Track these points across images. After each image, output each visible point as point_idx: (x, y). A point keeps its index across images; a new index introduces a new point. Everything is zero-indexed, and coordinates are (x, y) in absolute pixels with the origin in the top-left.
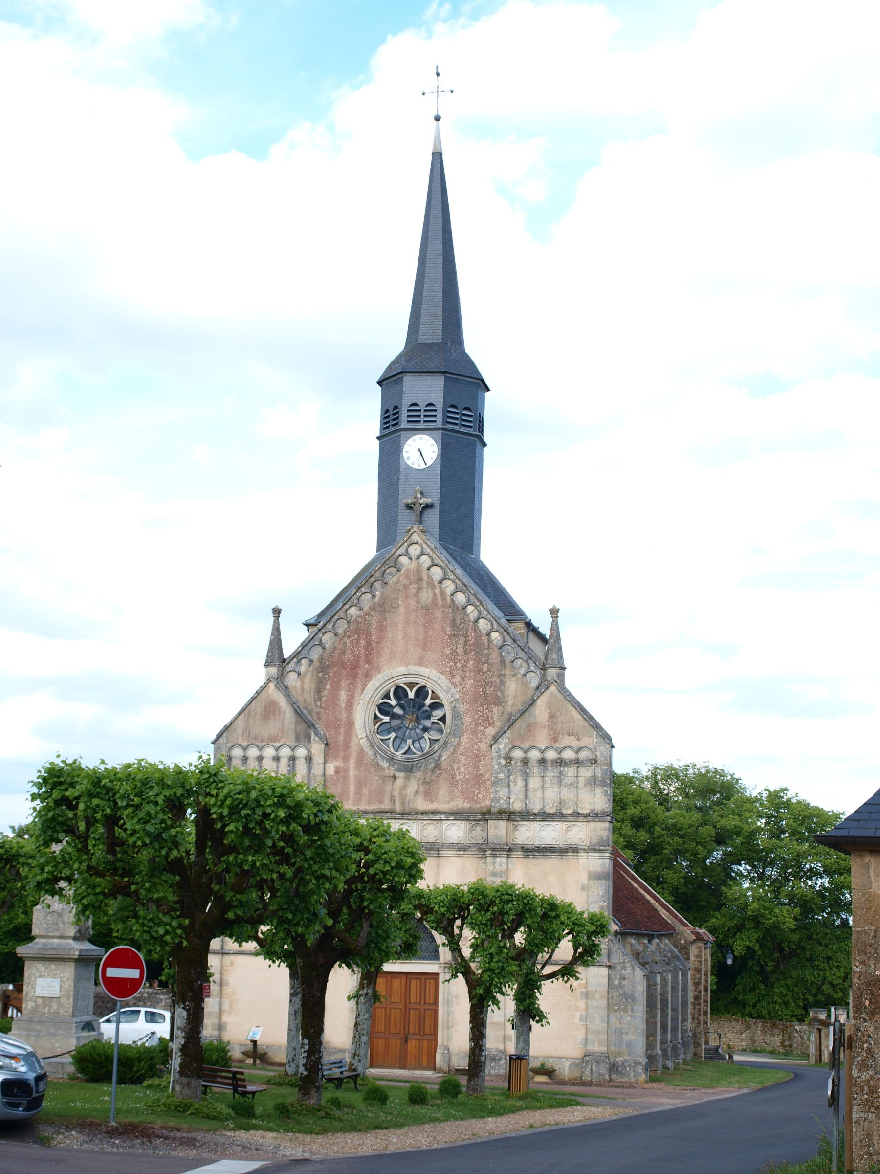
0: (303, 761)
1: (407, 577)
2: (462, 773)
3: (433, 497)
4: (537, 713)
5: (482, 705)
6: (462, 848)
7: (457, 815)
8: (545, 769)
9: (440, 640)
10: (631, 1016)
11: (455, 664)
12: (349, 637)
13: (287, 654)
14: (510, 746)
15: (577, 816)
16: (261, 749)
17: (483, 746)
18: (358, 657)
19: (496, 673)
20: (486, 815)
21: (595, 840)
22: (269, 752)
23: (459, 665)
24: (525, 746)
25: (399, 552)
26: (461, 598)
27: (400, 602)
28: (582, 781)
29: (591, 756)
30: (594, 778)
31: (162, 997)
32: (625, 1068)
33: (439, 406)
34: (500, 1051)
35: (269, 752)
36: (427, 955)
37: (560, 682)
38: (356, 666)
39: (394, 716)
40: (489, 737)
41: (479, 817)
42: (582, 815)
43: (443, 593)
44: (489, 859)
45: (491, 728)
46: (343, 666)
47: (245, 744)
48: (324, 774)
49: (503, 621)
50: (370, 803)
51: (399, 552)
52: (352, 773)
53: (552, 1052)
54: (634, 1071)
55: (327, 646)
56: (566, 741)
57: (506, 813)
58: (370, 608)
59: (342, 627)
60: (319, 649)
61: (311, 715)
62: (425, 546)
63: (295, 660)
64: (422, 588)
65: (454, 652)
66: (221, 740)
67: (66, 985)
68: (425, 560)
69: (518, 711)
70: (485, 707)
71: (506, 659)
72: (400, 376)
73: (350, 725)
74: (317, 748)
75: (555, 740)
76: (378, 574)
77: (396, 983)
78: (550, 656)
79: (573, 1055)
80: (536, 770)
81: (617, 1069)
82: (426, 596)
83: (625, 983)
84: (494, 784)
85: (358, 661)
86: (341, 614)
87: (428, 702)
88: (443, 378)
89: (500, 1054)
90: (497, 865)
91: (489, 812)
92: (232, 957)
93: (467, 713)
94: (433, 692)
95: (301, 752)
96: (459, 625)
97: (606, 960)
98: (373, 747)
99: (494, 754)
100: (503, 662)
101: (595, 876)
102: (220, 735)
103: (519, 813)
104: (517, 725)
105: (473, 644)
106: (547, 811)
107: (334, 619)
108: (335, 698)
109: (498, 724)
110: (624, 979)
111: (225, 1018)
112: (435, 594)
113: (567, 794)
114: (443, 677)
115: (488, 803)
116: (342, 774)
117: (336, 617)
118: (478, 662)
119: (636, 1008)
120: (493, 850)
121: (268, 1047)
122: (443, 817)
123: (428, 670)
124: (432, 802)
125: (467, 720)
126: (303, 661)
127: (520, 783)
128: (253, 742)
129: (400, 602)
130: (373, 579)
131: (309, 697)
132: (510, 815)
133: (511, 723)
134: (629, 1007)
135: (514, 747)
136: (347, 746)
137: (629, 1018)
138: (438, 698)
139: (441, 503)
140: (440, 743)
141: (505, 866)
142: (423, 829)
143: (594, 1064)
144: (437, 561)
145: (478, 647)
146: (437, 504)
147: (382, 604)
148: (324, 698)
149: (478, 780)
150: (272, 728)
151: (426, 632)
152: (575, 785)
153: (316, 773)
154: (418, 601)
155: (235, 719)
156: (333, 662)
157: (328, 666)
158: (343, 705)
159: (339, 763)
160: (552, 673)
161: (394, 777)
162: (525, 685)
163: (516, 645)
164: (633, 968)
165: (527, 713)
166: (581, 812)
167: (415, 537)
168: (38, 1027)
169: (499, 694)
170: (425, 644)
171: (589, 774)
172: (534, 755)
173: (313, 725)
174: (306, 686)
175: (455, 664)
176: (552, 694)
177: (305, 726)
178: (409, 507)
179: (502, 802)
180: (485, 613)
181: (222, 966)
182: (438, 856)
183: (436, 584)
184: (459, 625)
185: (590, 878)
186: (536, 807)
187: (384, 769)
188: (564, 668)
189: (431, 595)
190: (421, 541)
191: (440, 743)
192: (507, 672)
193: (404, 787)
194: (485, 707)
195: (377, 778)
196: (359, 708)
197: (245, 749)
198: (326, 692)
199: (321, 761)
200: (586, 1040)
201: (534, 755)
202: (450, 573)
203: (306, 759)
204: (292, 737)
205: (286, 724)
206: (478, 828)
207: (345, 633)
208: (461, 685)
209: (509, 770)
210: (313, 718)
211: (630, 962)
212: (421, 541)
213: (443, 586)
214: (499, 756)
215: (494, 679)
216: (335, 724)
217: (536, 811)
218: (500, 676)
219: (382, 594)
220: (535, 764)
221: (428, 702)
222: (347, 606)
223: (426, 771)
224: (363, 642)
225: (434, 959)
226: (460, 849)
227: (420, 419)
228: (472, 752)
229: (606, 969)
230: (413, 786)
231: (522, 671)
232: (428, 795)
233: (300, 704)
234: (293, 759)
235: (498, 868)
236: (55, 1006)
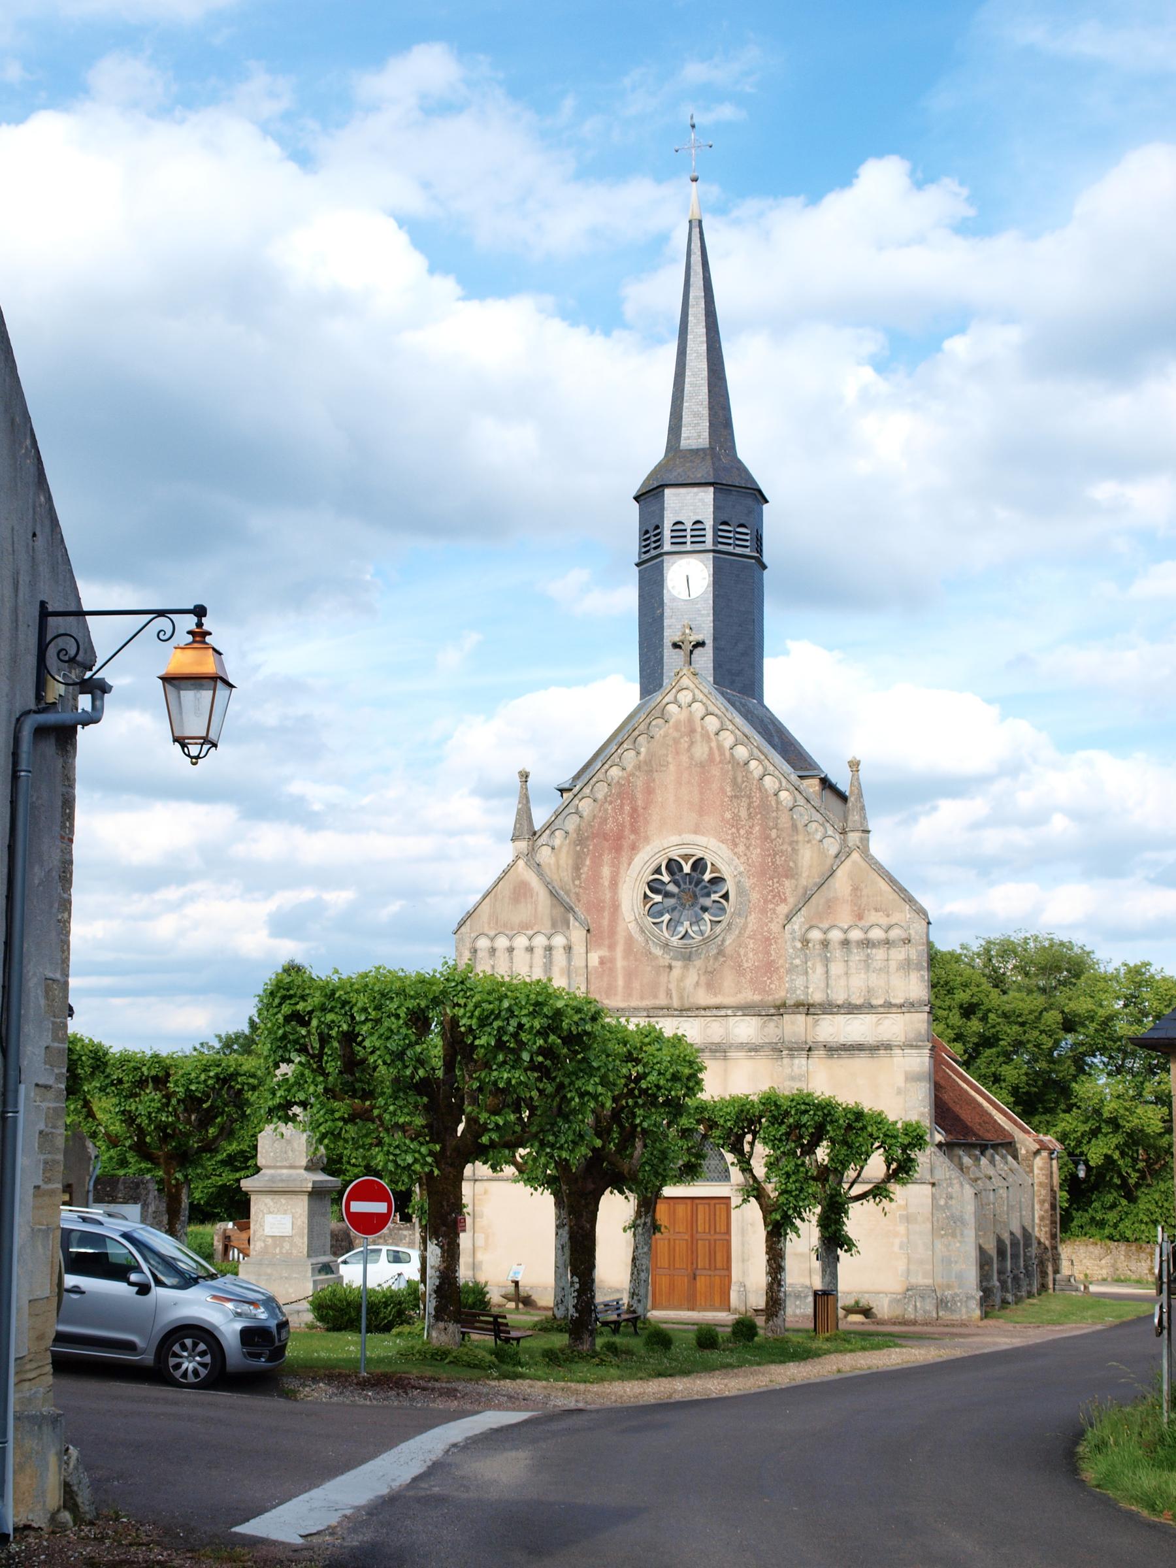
0: (561, 951)
1: (677, 728)
2: (750, 959)
3: (705, 631)
4: (837, 885)
5: (771, 878)
6: (753, 1049)
7: (747, 1010)
8: (849, 951)
11: (738, 830)
12: (611, 803)
14: (807, 926)
15: (888, 1005)
17: (775, 927)
18: (623, 825)
20: (780, 1009)
21: (912, 1035)
22: (521, 942)
24: (825, 925)
26: (742, 752)
27: (670, 759)
28: (893, 965)
29: (904, 935)
30: (908, 961)
31: (405, 1233)
32: (955, 1303)
33: (709, 524)
35: (521, 942)
37: (864, 850)
38: (620, 837)
39: (667, 895)
41: (772, 1011)
42: (895, 1005)
43: (720, 747)
44: (786, 1061)
45: (783, 905)
46: (605, 837)
47: (492, 933)
49: (794, 777)
50: (642, 998)
52: (620, 963)
54: (967, 1307)
55: (585, 814)
56: (873, 917)
57: (803, 1005)
58: (634, 767)
59: (601, 791)
62: (697, 691)
65: (736, 817)
66: (463, 929)
67: (299, 1222)
69: (815, 884)
73: (616, 907)
74: (577, 935)
75: (860, 917)
76: (642, 727)
77: (681, 1209)
82: (701, 751)
83: (953, 1202)
84: (789, 971)
85: (623, 830)
86: (600, 775)
87: (707, 876)
90: (795, 1068)
91: (784, 1005)
95: (559, 941)
97: (928, 1177)
98: (643, 932)
99: (787, 936)
100: (794, 827)
101: (911, 1078)
102: (462, 924)
105: (758, 806)
107: (592, 782)
108: (596, 877)
110: (951, 1198)
111: (480, 1256)
112: (711, 749)
113: (875, 980)
114: (723, 846)
115: (783, 994)
116: (608, 965)
117: (594, 779)
118: (765, 828)
119: (966, 1232)
120: (791, 1050)
122: (729, 1012)
124: (715, 995)
125: (755, 896)
126: (557, 833)
127: (820, 969)
130: (636, 733)
131: (566, 875)
132: (808, 1008)
134: (958, 1231)
135: (811, 927)
136: (612, 932)
138: (718, 871)
139: (715, 639)
141: (804, 1068)
142: (706, 1027)
144: (712, 708)
145: (764, 808)
147: (648, 763)
149: (769, 967)
150: (523, 913)
151: (701, 793)
152: (885, 970)
154: (691, 758)
158: (607, 884)
160: (854, 838)
162: (822, 853)
164: (962, 1185)
165: (825, 886)
166: (894, 1001)
167: (685, 681)
168: (269, 1271)
169: (791, 864)
172: (836, 935)
173: (572, 908)
174: (562, 862)
175: (738, 830)
176: (854, 863)
177: (562, 909)
178: (676, 646)
179: (798, 992)
180: (772, 768)
182: (725, 1058)
184: (740, 785)
185: (907, 1079)
186: (839, 997)
188: (868, 832)
189: (706, 749)
190: (692, 686)
191: (724, 925)
192: (801, 838)
193: (682, 979)
195: (649, 968)
197: (492, 939)
198: (586, 869)
199: (583, 950)
200: (908, 1271)
201: (836, 935)
202: (728, 723)
204: (548, 924)
205: (540, 908)
206: (772, 1025)
209: (806, 955)
210: (571, 900)
211: (958, 1178)
212: (692, 686)
213: (721, 738)
214: (794, 939)
216: (596, 907)
217: (839, 1002)
218: (791, 843)
219: (648, 749)
220: (837, 946)
221: (707, 876)
222: (606, 766)
223: (707, 958)
224: (627, 808)
227: (687, 538)
230: (692, 977)
231: (819, 836)
232: (710, 986)
233: (555, 884)
234: (549, 949)
236: (287, 1246)
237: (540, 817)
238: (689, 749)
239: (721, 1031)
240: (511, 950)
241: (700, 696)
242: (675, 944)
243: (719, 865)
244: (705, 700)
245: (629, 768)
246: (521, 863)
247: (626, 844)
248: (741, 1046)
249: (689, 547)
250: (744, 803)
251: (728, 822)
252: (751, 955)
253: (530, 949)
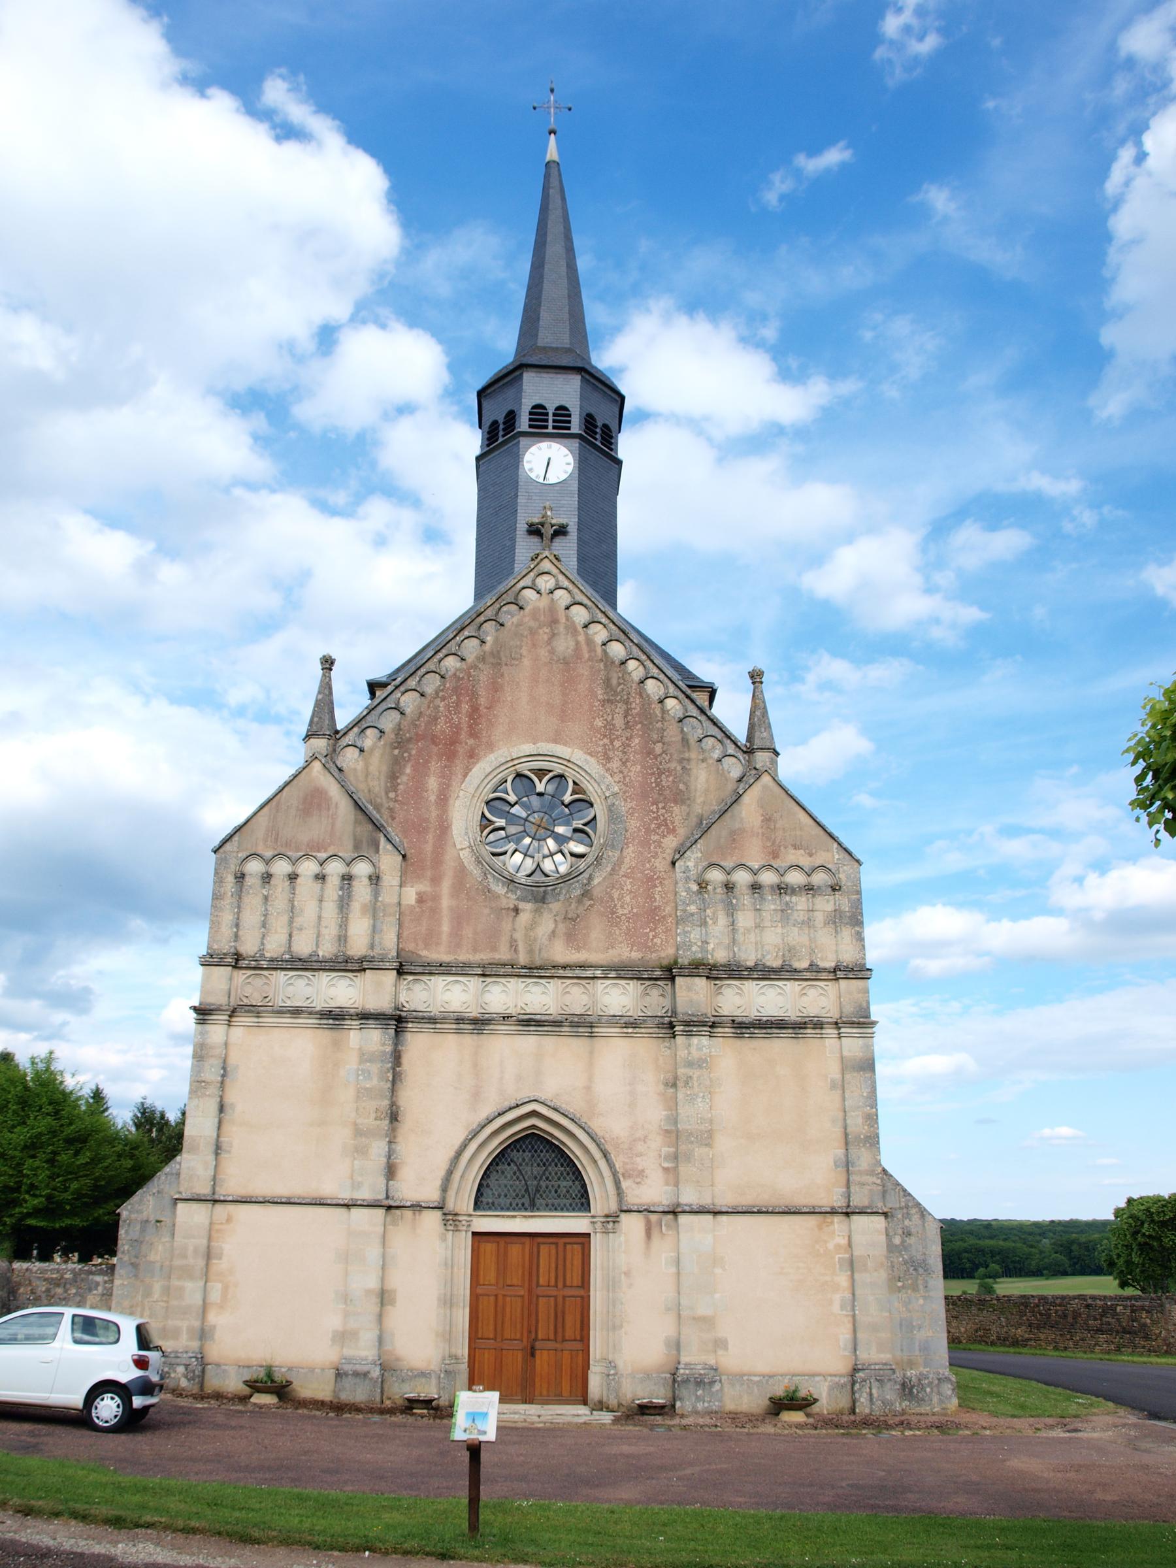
0: (366, 881)
1: (535, 619)
4: (744, 814)
5: (655, 803)
6: (631, 1024)
7: (623, 972)
8: (762, 898)
9: (586, 707)
10: (925, 1298)
11: (612, 742)
13: (341, 723)
14: (705, 864)
16: (294, 862)
17: (661, 864)
19: (675, 756)
20: (670, 973)
22: (308, 868)
24: (729, 864)
25: (522, 584)
27: (524, 651)
28: (819, 917)
31: (99, 1278)
32: (923, 1389)
34: (712, 1369)
35: (308, 868)
36: (567, 1202)
38: (453, 741)
39: (512, 819)
40: (668, 851)
41: (658, 973)
42: (825, 970)
43: (590, 642)
46: (434, 740)
47: (268, 854)
48: (399, 904)
50: (475, 950)
51: (522, 584)
52: (446, 902)
53: (797, 1365)
54: (939, 1393)
55: (408, 711)
58: (478, 658)
60: (395, 715)
61: (379, 811)
62: (561, 577)
63: (356, 730)
64: (558, 634)
66: (228, 847)
68: (562, 597)
69: (714, 812)
71: (690, 737)
72: (517, 373)
73: (444, 828)
74: (389, 861)
75: (775, 855)
77: (515, 1250)
78: (757, 734)
79: (832, 1370)
80: (747, 900)
81: (911, 1392)
82: (564, 645)
83: (911, 1241)
85: (458, 733)
86: (431, 666)
88: (579, 377)
89: (712, 1373)
90: (693, 1050)
92: (231, 1208)
94: (575, 783)
95: (362, 869)
96: (614, 689)
97: (880, 1204)
98: (480, 862)
100: (685, 741)
103: (724, 966)
104: (713, 831)
106: (768, 964)
108: (418, 789)
109: (682, 832)
110: (909, 1234)
111: (212, 1318)
112: (577, 643)
113: (796, 937)
114: (593, 760)
115: (671, 951)
116: (430, 904)
117: (423, 670)
119: (931, 1283)
121: (290, 1369)
124: (578, 949)
125: (633, 824)
126: (369, 732)
127: (722, 920)
128: (283, 851)
130: (482, 618)
133: (704, 828)
134: (920, 1282)
135: (711, 865)
136: (438, 861)
137: (921, 1301)
140: (589, 859)
143: (875, 1385)
144: (580, 597)
145: (647, 718)
146: (573, 529)
147: (496, 654)
148: (401, 787)
149: (653, 915)
150: (316, 829)
152: (808, 923)
153: (387, 900)
154: (552, 652)
155: (255, 814)
156: (417, 734)
157: (409, 740)
158: (433, 798)
159: (424, 887)
160: (761, 758)
161: (516, 910)
162: (722, 776)
163: (703, 718)
166: (822, 964)
169: (681, 786)
170: (563, 711)
171: (830, 907)
174: (373, 769)
175: (612, 742)
176: (765, 787)
177: (370, 827)
179: (694, 948)
181: (211, 1224)
182: (591, 1036)
183: (580, 629)
189: (572, 644)
190: (555, 571)
194: (660, 805)
195: (487, 911)
196: (458, 803)
198: (404, 779)
199: (396, 882)
201: (742, 878)
203: (370, 878)
204: (349, 844)
205: (339, 824)
206: (655, 992)
207: (437, 693)
208: (621, 772)
214: (688, 879)
216: (418, 828)
217: (750, 964)
218: (681, 761)
219: (496, 639)
220: (745, 890)
222: (440, 655)
224: (465, 707)
225: (580, 1210)
226: (627, 1025)
228: (642, 872)
229: (882, 1218)
230: (546, 925)
231: (717, 754)
232: (571, 938)
234: (347, 878)
235: (695, 1054)
237: (343, 719)
239: (585, 999)
240: (293, 877)
241: (566, 583)
242: (523, 881)
243: (585, 784)
244: (571, 587)
245: (471, 658)
246: (317, 765)
247: (461, 750)
248: (616, 1020)
249: (550, 430)
250: (620, 709)
251: (598, 731)
252: (628, 899)
253: (321, 878)
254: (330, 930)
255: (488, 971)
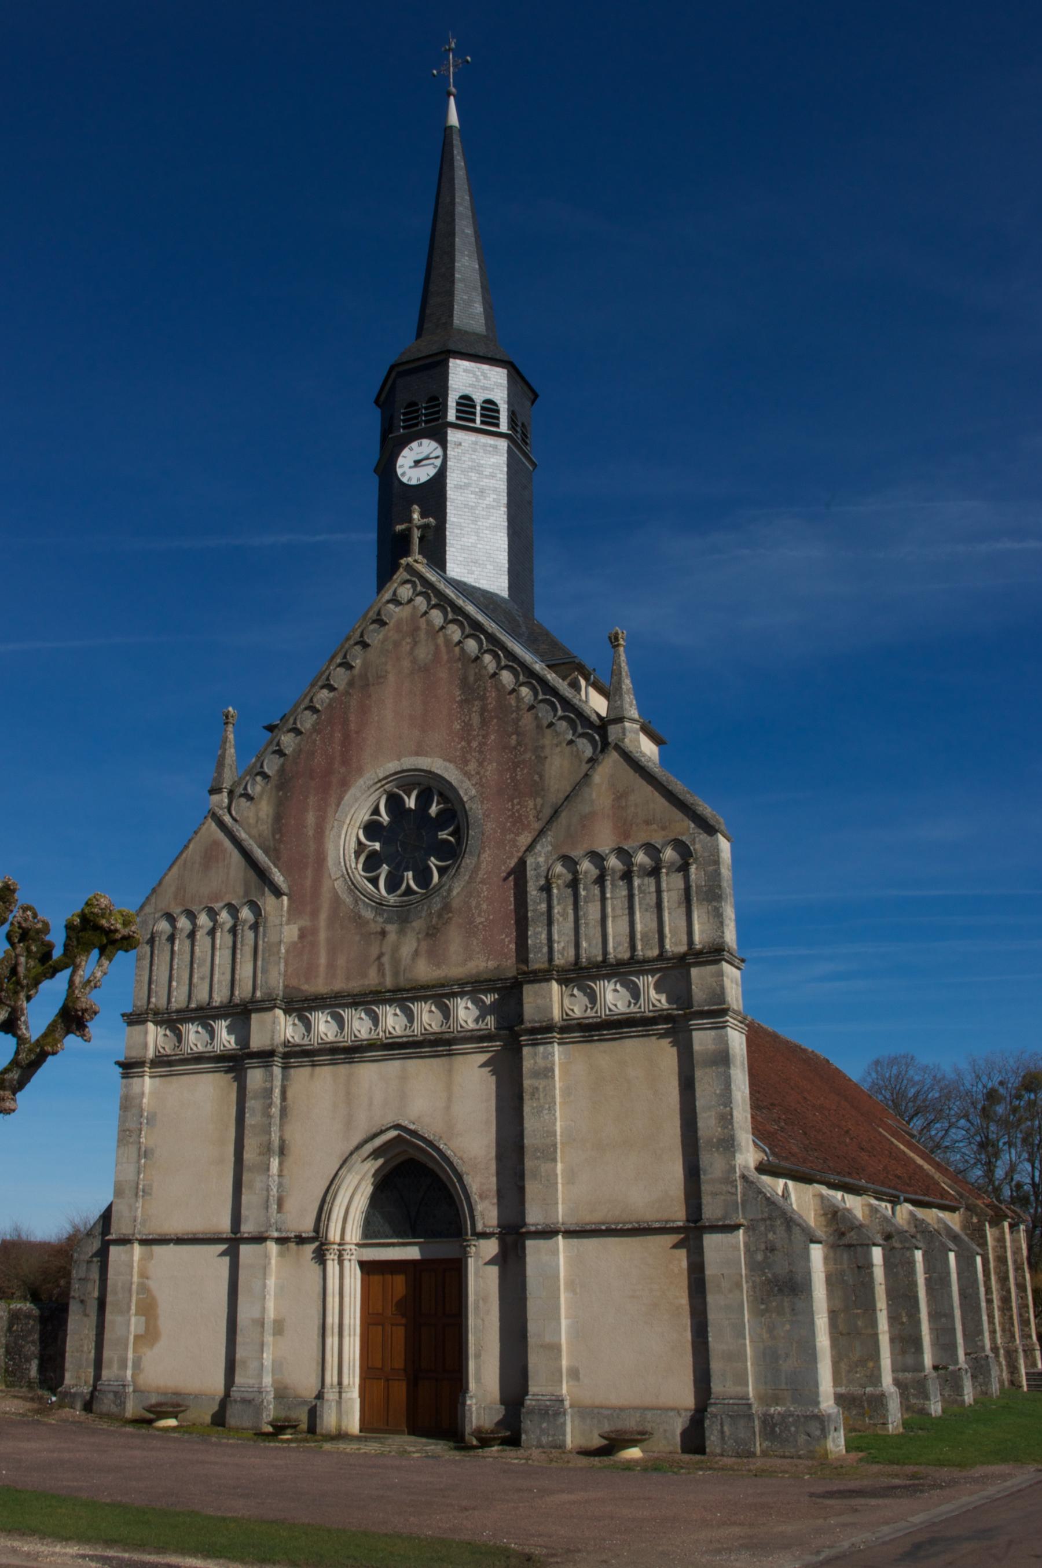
5: (511, 799)
11: (469, 743)
23: (474, 744)
27: (389, 668)
52: (323, 935)
65: (467, 727)
70: (515, 801)
81: (773, 1431)
93: (488, 816)
112: (437, 646)
114: (451, 766)
123: (430, 760)
129: (389, 668)
137: (788, 1327)
143: (727, 1422)
147: (364, 676)
154: (414, 661)
158: (311, 833)
161: (383, 933)
162: (577, 755)
175: (469, 743)
187: (368, 922)
194: (515, 801)
208: (478, 773)
215: (528, 756)
232: (435, 956)
238: (411, 652)
252: (484, 906)
254: (221, 977)
255: (367, 1000)
